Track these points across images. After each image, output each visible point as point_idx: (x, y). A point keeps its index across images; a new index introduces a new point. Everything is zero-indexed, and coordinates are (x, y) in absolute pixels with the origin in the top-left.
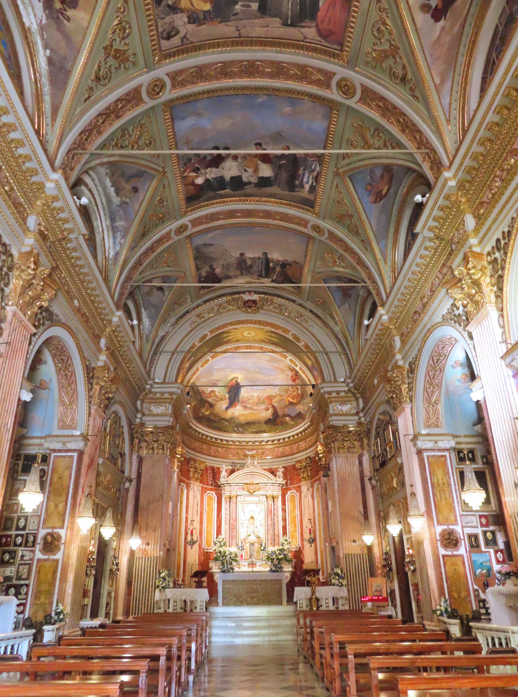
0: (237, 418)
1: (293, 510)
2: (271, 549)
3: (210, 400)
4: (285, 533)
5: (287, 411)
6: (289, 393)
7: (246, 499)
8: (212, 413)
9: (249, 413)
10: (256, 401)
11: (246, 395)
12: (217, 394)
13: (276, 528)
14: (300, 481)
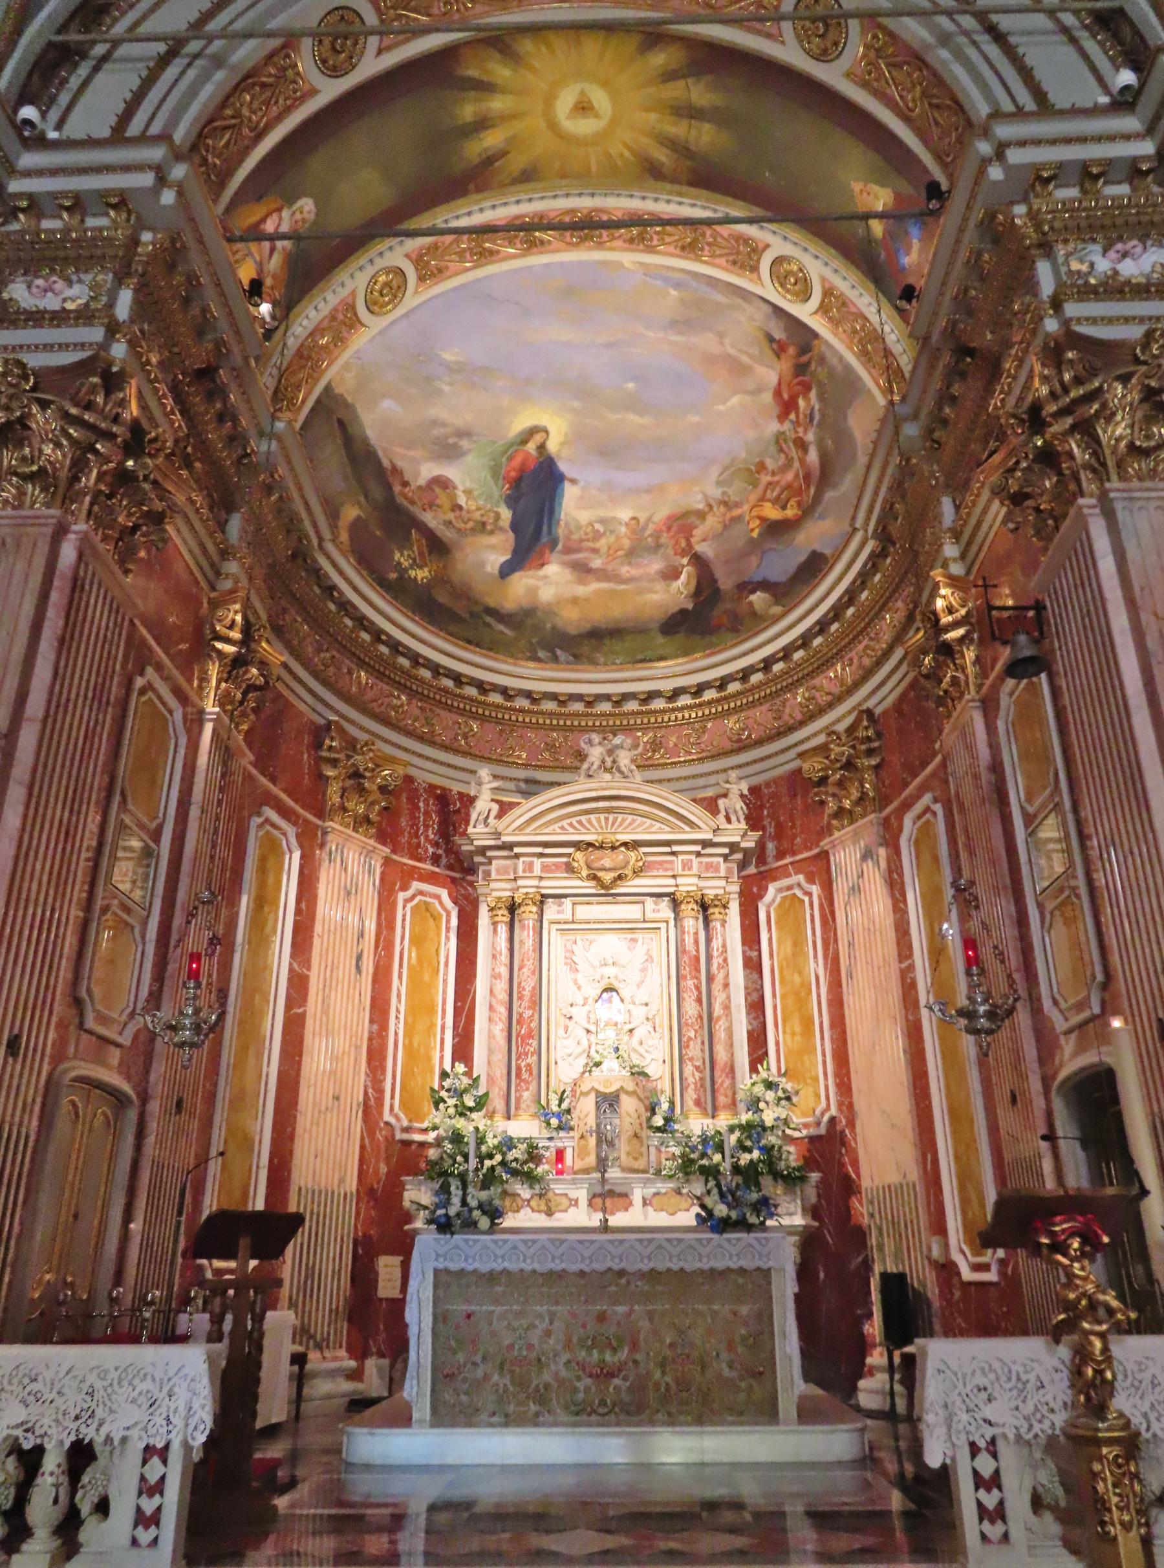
0: (550, 611)
1: (795, 961)
2: (696, 1125)
3: (429, 519)
4: (758, 1053)
5: (755, 568)
6: (765, 479)
7: (583, 912)
8: (441, 580)
9: (599, 593)
10: (626, 543)
11: (584, 516)
12: (462, 500)
13: (721, 1034)
14: (828, 830)
